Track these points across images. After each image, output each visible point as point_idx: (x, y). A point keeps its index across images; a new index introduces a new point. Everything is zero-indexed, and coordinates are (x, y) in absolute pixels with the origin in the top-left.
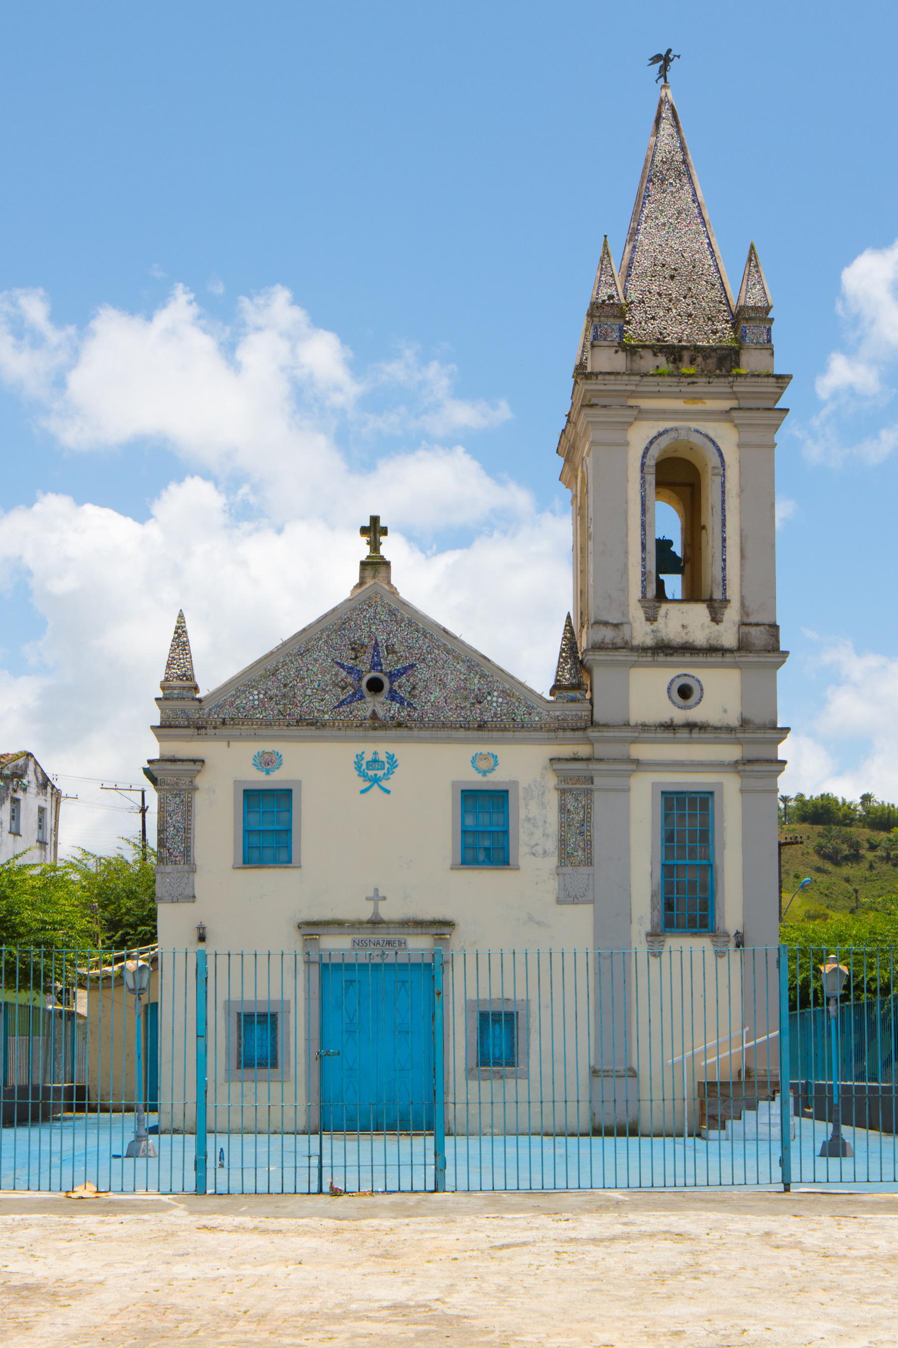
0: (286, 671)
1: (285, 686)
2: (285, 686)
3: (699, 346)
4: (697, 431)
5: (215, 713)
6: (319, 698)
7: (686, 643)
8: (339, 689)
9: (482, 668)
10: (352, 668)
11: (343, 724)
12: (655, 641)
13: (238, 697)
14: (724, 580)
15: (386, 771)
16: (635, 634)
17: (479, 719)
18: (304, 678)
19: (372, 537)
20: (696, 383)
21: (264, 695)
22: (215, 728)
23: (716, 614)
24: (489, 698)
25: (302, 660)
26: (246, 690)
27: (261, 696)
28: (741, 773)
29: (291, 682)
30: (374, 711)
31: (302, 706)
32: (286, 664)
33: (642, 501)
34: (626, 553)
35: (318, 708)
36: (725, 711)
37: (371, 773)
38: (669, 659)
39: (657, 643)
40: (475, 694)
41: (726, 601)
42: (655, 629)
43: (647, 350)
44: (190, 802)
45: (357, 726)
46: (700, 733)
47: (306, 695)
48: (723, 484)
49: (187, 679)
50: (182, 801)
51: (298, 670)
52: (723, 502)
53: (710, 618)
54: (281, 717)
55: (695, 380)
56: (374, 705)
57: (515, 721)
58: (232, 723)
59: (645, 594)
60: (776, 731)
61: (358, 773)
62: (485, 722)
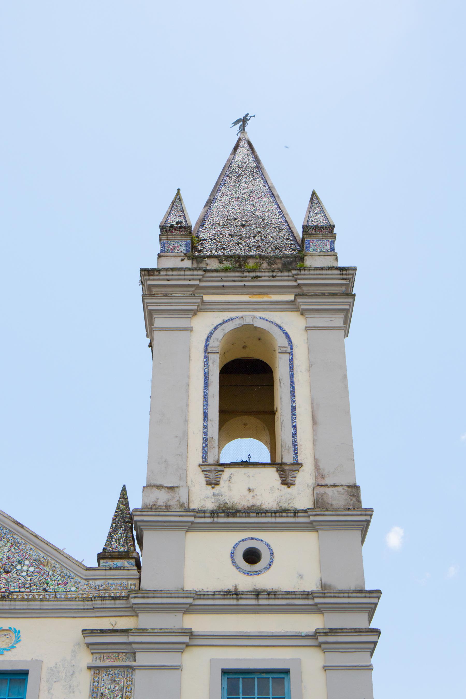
3: (264, 255)
4: (263, 319)
7: (253, 506)
9: (14, 536)
12: (217, 505)
14: (295, 444)
16: (193, 498)
17: (3, 590)
20: (260, 277)
23: (286, 477)
24: (19, 567)
28: (323, 646)
33: (205, 377)
34: (186, 421)
36: (301, 577)
38: (231, 520)
39: (219, 507)
40: (3, 562)
41: (297, 465)
42: (217, 492)
43: (213, 259)
46: (269, 599)
48: (291, 361)
52: (292, 376)
53: (280, 482)
55: (259, 274)
57: (46, 591)
59: (206, 460)
60: (363, 595)
62: (10, 593)
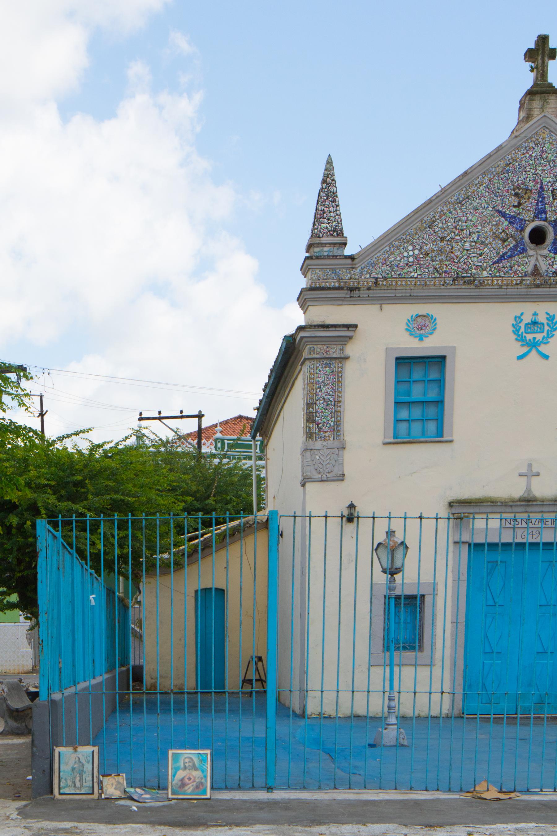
0: (444, 222)
1: (442, 239)
2: (442, 239)
5: (367, 273)
6: (478, 252)
8: (500, 242)
10: (514, 217)
11: (502, 281)
13: (392, 253)
15: (545, 334)
18: (462, 230)
19: (540, 61)
21: (419, 250)
22: (369, 289)
25: (461, 209)
26: (401, 246)
27: (416, 252)
29: (448, 235)
30: (535, 266)
31: (459, 262)
32: (444, 214)
35: (476, 264)
37: (529, 337)
44: (341, 372)
45: (517, 284)
47: (464, 250)
49: (338, 235)
50: (332, 372)
51: (457, 221)
54: (436, 274)
56: (537, 259)
58: (385, 283)
61: (516, 337)
